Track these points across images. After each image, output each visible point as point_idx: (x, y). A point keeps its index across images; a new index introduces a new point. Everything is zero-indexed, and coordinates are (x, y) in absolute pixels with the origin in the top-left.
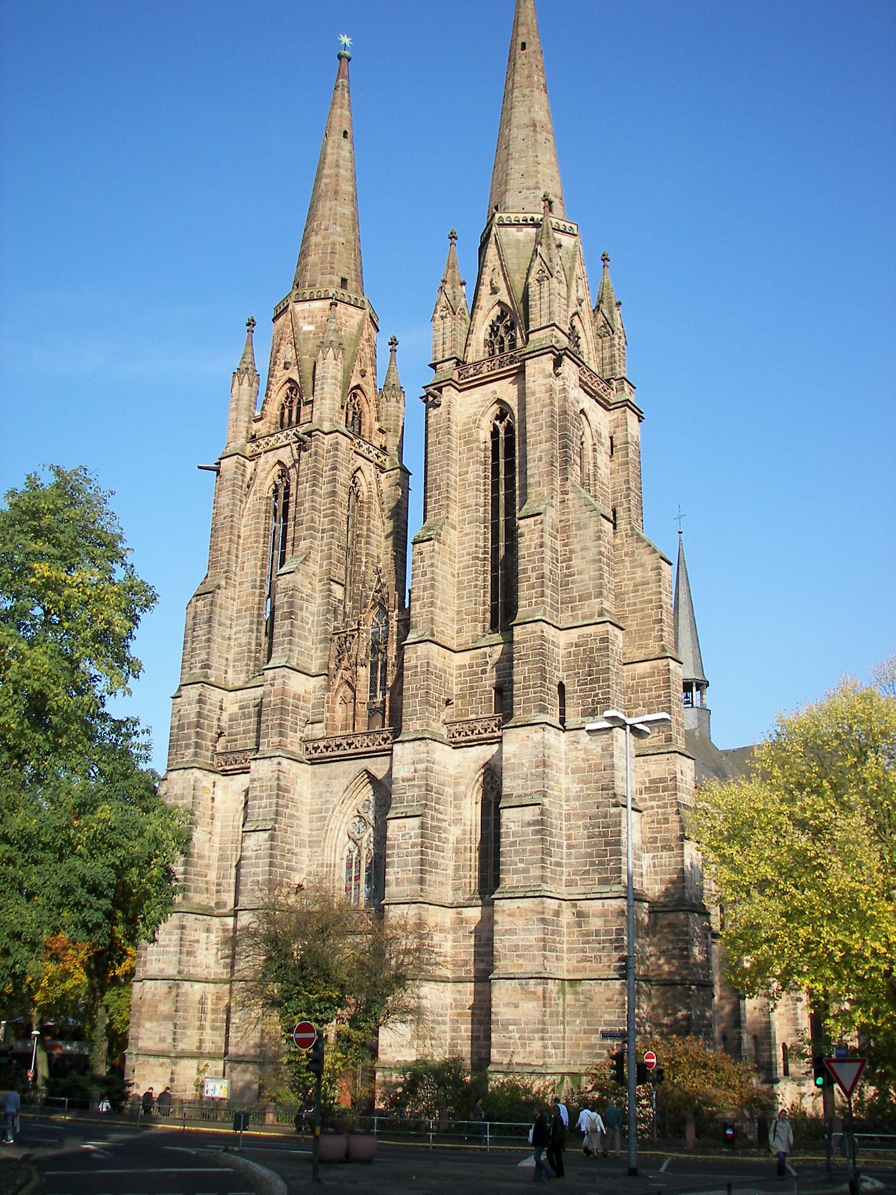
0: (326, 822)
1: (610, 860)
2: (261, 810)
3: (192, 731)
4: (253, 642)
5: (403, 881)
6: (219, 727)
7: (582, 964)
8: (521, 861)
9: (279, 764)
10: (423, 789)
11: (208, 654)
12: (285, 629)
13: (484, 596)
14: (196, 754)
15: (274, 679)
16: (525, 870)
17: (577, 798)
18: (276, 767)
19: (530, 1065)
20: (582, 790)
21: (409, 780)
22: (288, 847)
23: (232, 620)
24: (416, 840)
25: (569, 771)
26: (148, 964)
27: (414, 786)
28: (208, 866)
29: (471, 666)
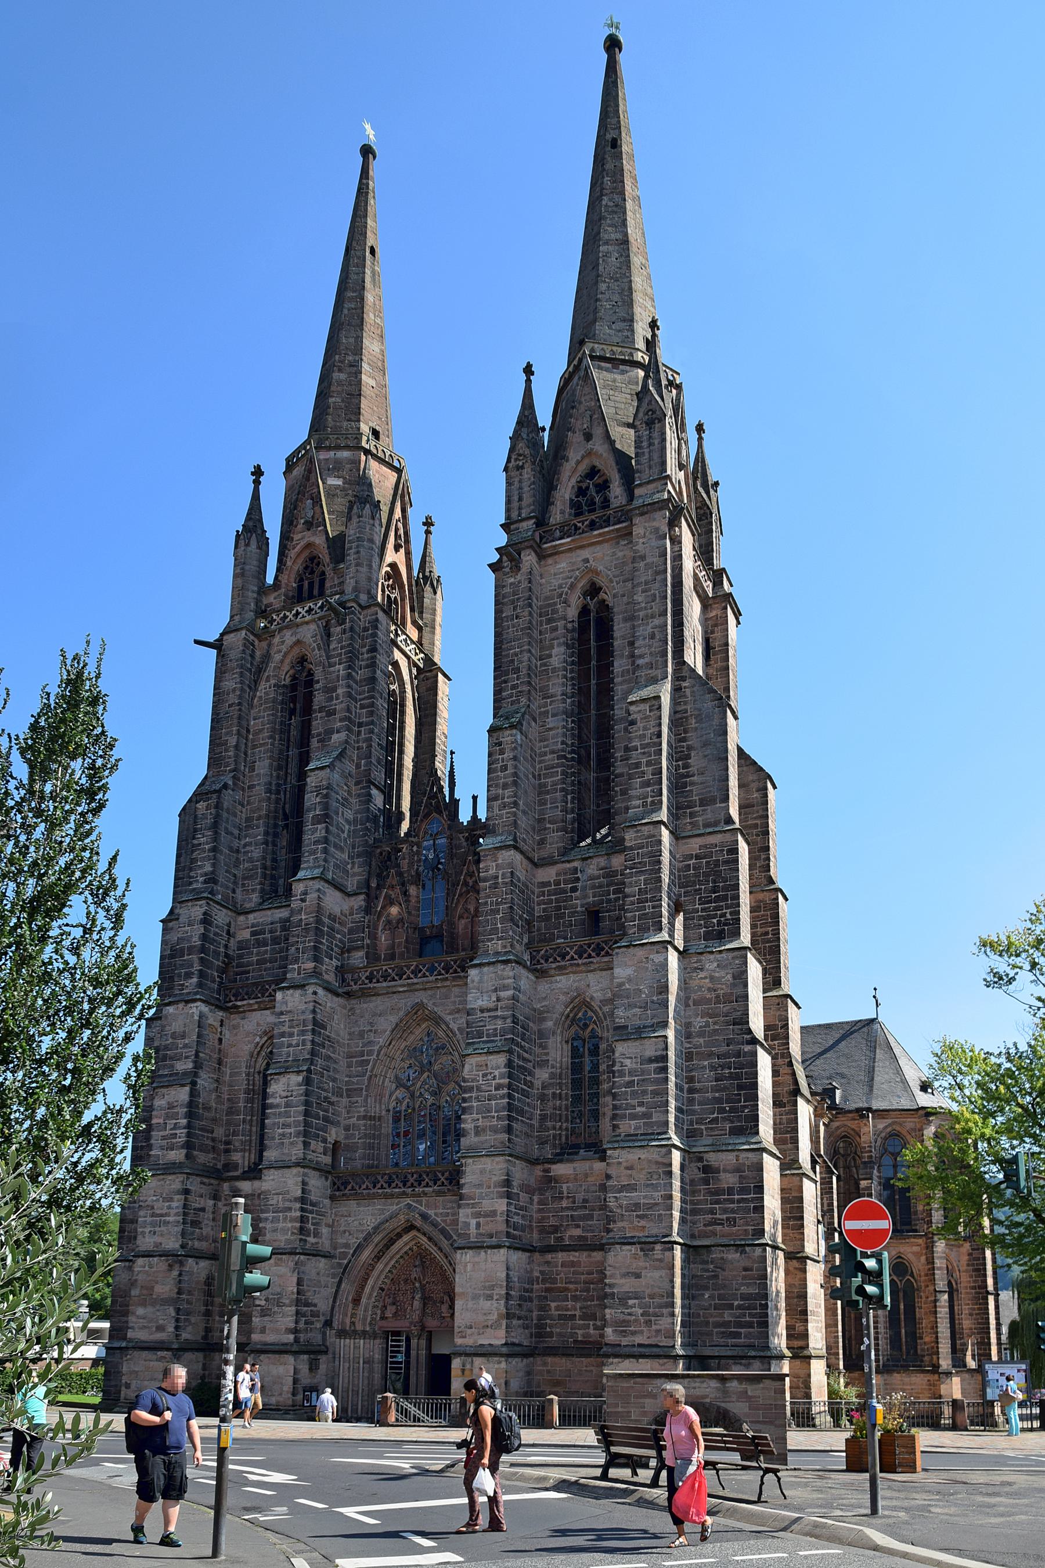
0: (369, 1067)
1: (745, 1107)
2: (291, 1049)
3: (195, 958)
4: (269, 857)
5: (484, 1130)
6: (227, 955)
7: (710, 1228)
8: (641, 1104)
9: (315, 993)
10: (509, 1020)
11: (214, 865)
12: (318, 835)
13: (572, 802)
14: (200, 985)
15: (305, 893)
16: (647, 1115)
17: (701, 1034)
18: (311, 997)
19: (657, 1346)
20: (707, 1025)
21: (489, 1010)
22: (324, 1094)
23: (240, 830)
24: (502, 1081)
25: (691, 1003)
26: (139, 1237)
27: (496, 1017)
28: (214, 1120)
29: (557, 883)
